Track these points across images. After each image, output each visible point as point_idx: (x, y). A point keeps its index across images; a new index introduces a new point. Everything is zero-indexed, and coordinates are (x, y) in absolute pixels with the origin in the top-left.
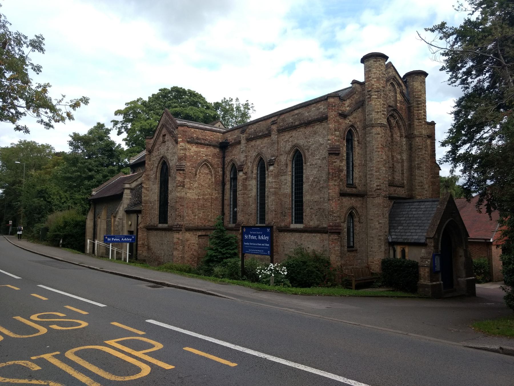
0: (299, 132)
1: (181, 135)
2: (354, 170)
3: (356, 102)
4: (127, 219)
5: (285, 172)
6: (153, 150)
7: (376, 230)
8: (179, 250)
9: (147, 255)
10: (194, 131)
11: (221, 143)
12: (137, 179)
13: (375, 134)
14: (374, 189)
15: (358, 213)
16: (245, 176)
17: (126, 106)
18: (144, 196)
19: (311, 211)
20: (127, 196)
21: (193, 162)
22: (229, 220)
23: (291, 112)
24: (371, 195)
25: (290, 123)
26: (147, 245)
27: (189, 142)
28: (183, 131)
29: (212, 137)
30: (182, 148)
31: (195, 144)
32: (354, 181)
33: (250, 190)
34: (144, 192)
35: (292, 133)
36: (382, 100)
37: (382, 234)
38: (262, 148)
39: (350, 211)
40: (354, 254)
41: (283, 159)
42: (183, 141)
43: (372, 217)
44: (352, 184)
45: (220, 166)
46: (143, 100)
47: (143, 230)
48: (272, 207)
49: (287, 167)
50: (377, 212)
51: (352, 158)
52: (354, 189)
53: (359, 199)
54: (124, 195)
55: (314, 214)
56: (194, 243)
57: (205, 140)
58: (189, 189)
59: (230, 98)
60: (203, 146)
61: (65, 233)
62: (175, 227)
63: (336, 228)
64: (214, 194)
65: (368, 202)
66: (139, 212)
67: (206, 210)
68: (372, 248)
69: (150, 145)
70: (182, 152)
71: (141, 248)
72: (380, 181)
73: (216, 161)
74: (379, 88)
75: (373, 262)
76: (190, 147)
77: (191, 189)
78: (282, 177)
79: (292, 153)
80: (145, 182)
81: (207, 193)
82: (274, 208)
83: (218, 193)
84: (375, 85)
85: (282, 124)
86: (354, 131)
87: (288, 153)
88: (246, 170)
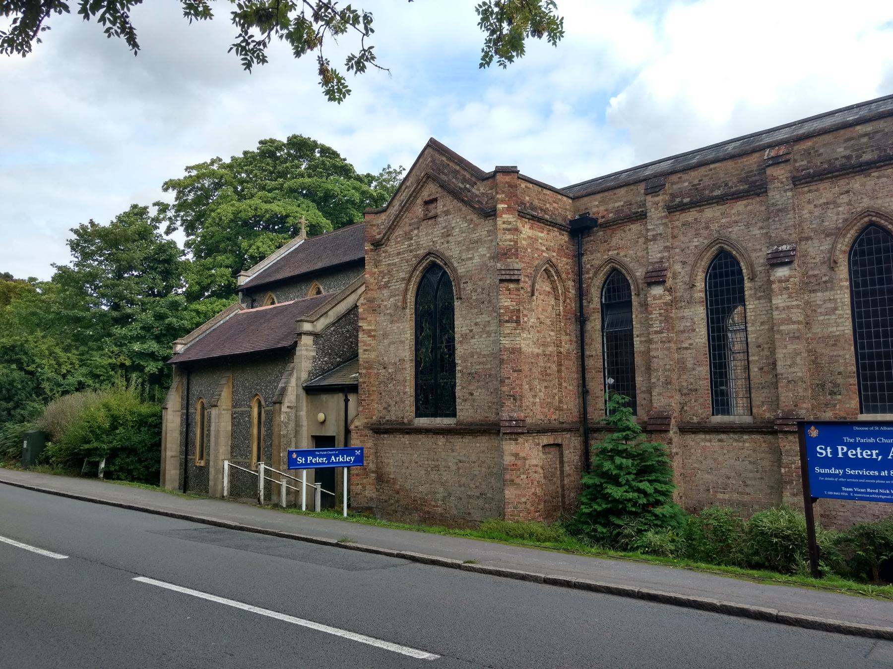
0: (878, 178)
1: (503, 196)
4: (307, 406)
5: (825, 282)
6: (388, 239)
9: (374, 496)
10: (526, 187)
11: (572, 222)
12: (327, 312)
17: (187, 174)
18: (365, 350)
20: (306, 350)
21: (526, 263)
22: (603, 408)
23: (842, 132)
25: (837, 159)
26: (374, 469)
28: (510, 186)
29: (555, 205)
30: (509, 227)
31: (529, 219)
33: (683, 332)
34: (363, 341)
35: (848, 184)
38: (729, 225)
41: (816, 249)
42: (509, 210)
46: (224, 163)
47: (363, 433)
48: (792, 370)
49: (832, 269)
54: (301, 350)
56: (537, 466)
59: (401, 167)
60: (542, 225)
61: (115, 443)
62: (507, 424)
66: (353, 388)
67: (551, 381)
69: (375, 228)
70: (509, 237)
71: (358, 478)
73: (564, 264)
76: (521, 225)
78: (813, 295)
79: (852, 232)
80: (364, 316)
85: (805, 163)
87: (838, 233)
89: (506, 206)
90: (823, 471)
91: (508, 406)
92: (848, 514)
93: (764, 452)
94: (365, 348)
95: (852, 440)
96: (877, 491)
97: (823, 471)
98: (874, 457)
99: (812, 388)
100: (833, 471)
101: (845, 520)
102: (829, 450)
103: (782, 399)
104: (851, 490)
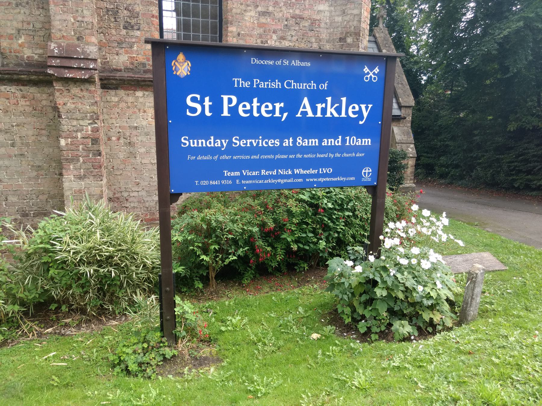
19: (263, 20)
55: (274, 32)
90: (194, 144)
92: (144, 193)
93: (23, 113)
95: (246, 85)
96: (275, 173)
97: (194, 144)
98: (277, 114)
99: (99, 15)
100: (212, 142)
101: (139, 202)
102: (207, 103)
103: (56, 24)
104: (238, 174)
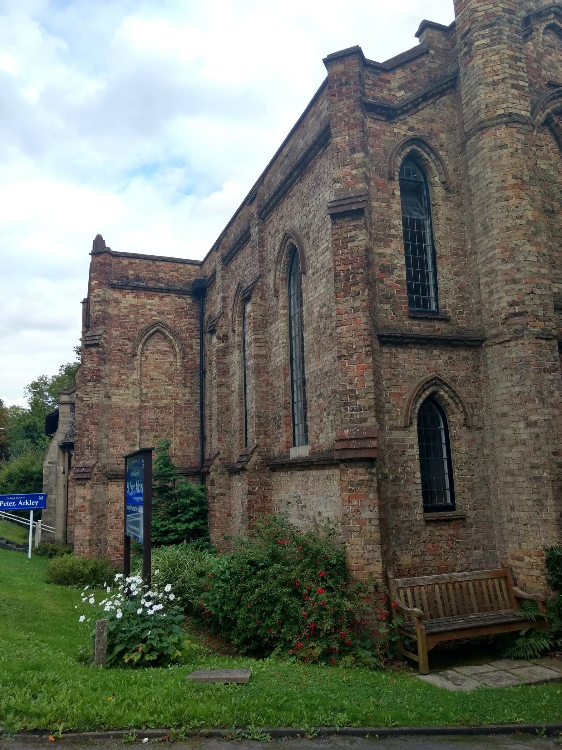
1: (95, 274)
2: (439, 268)
3: (430, 78)
7: (521, 448)
8: (84, 524)
10: (129, 262)
13: (492, 149)
14: (503, 316)
15: (458, 396)
16: (223, 344)
24: (496, 336)
27: (114, 287)
29: (175, 274)
30: (99, 299)
31: (132, 290)
32: (442, 302)
34: (78, 407)
36: (505, 46)
37: (544, 460)
39: (427, 393)
40: (452, 532)
43: (503, 405)
44: (437, 312)
45: (196, 333)
50: (517, 389)
51: (432, 237)
52: (438, 325)
53: (463, 353)
57: (158, 281)
58: (118, 386)
60: (152, 293)
63: (360, 444)
64: (180, 396)
65: (489, 361)
67: (164, 431)
68: (512, 509)
72: (520, 286)
74: (493, 14)
75: (521, 559)
77: (122, 386)
79: (284, 257)
80: (80, 386)
81: (164, 393)
82: (254, 409)
83: (193, 393)
84: (479, 9)
86: (426, 156)
88: (224, 330)
89: (97, 282)
91: (86, 455)
94: (79, 412)
